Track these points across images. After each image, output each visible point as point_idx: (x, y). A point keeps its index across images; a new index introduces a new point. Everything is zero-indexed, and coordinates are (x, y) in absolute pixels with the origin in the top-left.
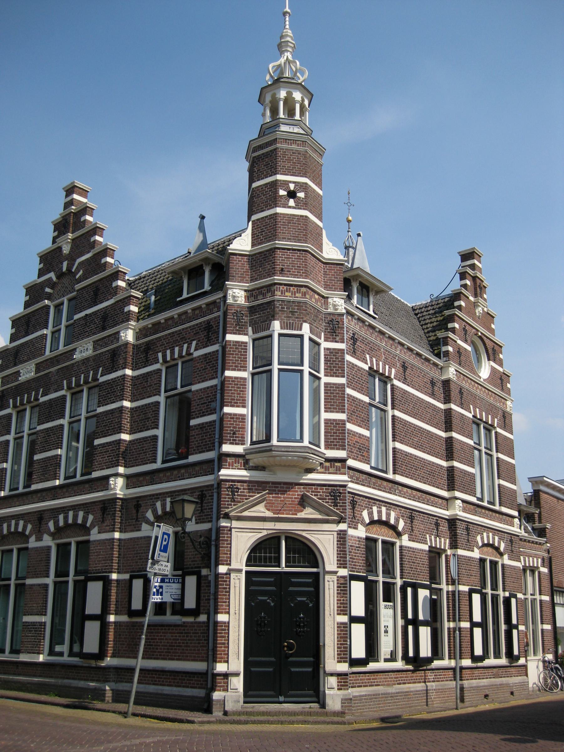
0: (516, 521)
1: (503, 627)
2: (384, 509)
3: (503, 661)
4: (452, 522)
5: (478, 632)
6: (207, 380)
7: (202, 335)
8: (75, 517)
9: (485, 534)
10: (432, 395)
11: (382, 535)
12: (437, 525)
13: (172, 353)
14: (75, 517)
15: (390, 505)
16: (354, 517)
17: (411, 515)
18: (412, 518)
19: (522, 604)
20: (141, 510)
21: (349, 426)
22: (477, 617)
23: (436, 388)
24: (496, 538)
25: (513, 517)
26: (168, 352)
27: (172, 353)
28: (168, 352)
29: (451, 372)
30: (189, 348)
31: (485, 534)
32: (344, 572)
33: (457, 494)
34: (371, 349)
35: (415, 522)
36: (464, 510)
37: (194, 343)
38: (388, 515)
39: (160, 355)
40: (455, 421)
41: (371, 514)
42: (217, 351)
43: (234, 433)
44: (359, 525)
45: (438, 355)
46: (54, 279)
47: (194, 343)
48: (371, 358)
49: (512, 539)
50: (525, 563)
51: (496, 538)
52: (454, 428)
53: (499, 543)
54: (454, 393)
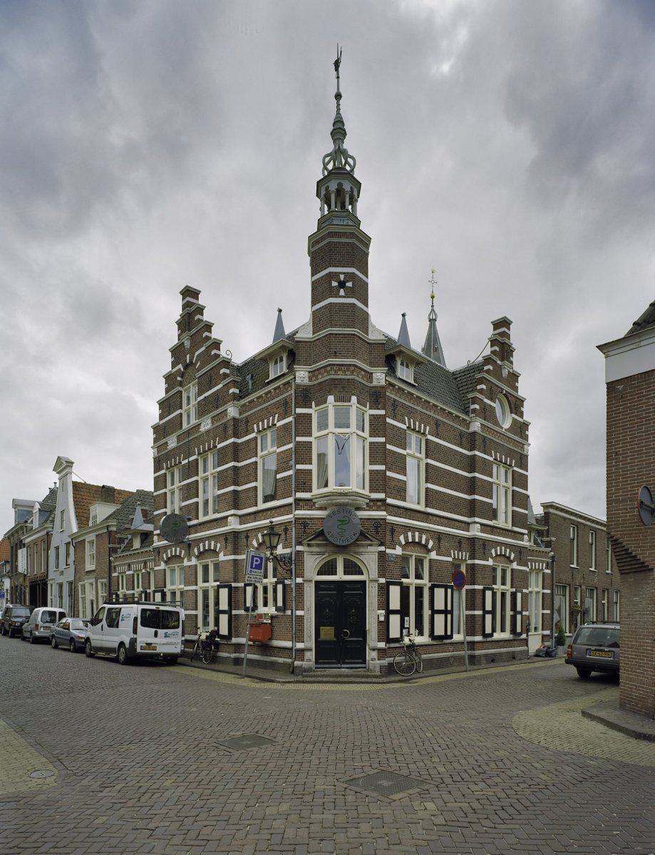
0: (526, 537)
1: (509, 613)
2: (417, 534)
3: (506, 635)
4: (472, 540)
5: (488, 618)
6: (286, 444)
7: (281, 410)
8: (210, 545)
9: (498, 548)
10: (461, 445)
11: (414, 554)
12: (460, 543)
13: (263, 424)
14: (210, 545)
15: (421, 531)
16: (393, 541)
17: (439, 537)
18: (439, 540)
19: (525, 596)
20: (249, 539)
21: (388, 473)
22: (489, 607)
23: (464, 439)
24: (508, 550)
25: (523, 534)
26: (260, 423)
27: (263, 424)
28: (260, 423)
29: (476, 426)
30: (273, 420)
31: (498, 548)
32: (383, 580)
33: (477, 520)
34: (410, 413)
35: (442, 542)
36: (482, 531)
37: (277, 416)
38: (420, 538)
39: (255, 426)
40: (478, 464)
41: (406, 538)
42: (292, 422)
43: (305, 484)
44: (397, 546)
45: (467, 413)
46: (182, 370)
47: (277, 416)
48: (409, 419)
49: (520, 551)
50: (532, 567)
51: (508, 550)
52: (477, 469)
53: (510, 554)
54: (479, 442)
